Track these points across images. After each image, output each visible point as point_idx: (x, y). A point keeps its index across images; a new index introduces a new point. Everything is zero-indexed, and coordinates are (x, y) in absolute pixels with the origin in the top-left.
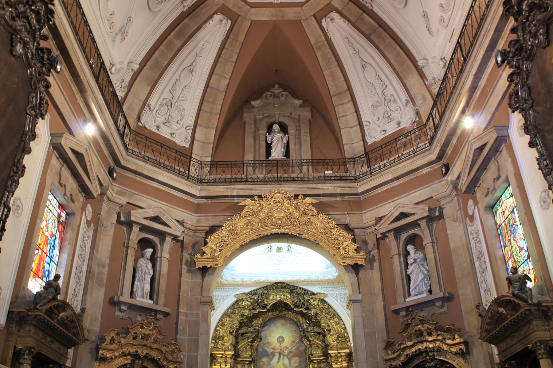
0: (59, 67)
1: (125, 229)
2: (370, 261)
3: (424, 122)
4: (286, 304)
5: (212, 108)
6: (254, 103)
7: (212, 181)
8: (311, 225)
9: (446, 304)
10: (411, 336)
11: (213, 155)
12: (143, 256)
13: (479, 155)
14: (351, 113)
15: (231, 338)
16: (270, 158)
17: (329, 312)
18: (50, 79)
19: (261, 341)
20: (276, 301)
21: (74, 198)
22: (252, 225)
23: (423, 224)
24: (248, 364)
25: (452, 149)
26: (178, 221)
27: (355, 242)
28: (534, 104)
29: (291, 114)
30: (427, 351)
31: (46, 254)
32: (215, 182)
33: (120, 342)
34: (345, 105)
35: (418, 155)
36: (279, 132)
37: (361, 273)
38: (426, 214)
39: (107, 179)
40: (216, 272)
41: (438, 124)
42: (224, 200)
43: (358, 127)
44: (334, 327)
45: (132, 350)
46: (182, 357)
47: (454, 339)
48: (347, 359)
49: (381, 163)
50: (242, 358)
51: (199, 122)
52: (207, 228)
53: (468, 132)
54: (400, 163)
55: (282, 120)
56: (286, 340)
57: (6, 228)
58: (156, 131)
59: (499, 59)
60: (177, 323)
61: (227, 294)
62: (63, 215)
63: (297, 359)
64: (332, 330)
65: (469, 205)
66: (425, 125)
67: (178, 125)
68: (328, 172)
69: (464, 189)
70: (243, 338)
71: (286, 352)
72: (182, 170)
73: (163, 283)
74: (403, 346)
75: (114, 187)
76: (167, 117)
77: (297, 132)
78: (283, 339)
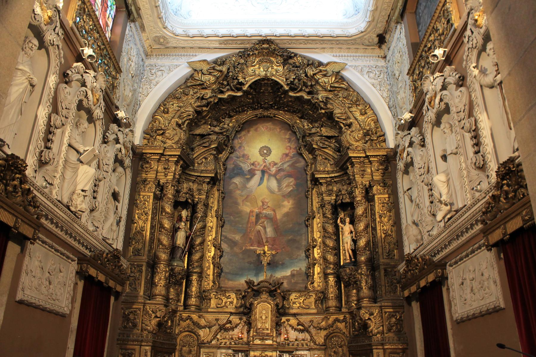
15: (178, 134)
17: (349, 95)
20: (259, 78)
24: (208, 183)
44: (356, 119)
48: (381, 167)
56: (274, 152)
64: (354, 125)
71: (273, 170)
78: (269, 151)
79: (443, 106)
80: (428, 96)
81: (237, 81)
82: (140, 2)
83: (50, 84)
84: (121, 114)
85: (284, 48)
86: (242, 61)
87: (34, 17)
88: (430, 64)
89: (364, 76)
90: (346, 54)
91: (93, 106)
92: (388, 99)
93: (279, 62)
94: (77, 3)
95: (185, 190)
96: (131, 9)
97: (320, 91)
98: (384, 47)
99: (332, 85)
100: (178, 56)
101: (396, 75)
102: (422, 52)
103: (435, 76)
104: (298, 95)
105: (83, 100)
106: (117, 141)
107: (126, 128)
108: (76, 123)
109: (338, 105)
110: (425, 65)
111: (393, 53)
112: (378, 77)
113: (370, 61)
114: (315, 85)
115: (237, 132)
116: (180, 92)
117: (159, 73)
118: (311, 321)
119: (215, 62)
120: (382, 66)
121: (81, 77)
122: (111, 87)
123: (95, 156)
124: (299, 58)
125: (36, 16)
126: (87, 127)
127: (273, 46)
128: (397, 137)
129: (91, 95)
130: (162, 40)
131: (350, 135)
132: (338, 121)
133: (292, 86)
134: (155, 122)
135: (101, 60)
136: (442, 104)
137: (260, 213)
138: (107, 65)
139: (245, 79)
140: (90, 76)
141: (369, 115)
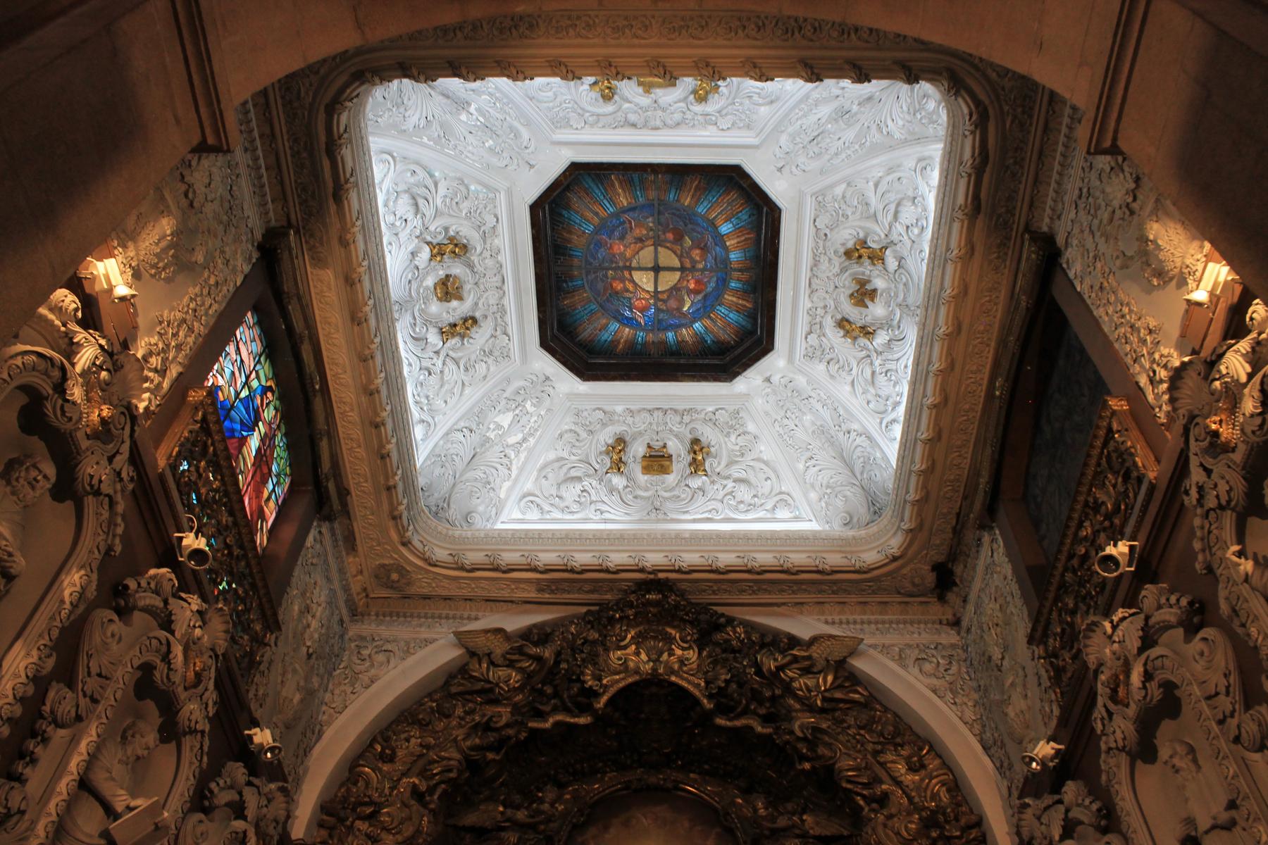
17: (872, 720)
20: (637, 678)
44: (898, 783)
79: (1156, 693)
80: (1103, 677)
81: (578, 685)
82: (350, 476)
83: (63, 591)
84: (262, 737)
85: (700, 604)
86: (594, 635)
87: (62, 407)
88: (1092, 598)
89: (909, 669)
90: (858, 618)
91: (180, 689)
92: (977, 727)
93: (689, 638)
94: (188, 424)
96: (327, 487)
97: (797, 711)
98: (950, 596)
99: (827, 694)
100: (433, 617)
101: (994, 658)
102: (1063, 575)
103: (1115, 619)
104: (738, 723)
105: (155, 668)
106: (238, 810)
107: (271, 780)
108: (125, 731)
109: (846, 747)
110: (1076, 605)
111: (978, 606)
112: (946, 670)
113: (920, 634)
114: (782, 696)
115: (575, 827)
116: (431, 708)
117: (381, 657)
119: (527, 635)
120: (953, 646)
121: (162, 605)
122: (246, 660)
123: (157, 827)
124: (738, 630)
125: (66, 405)
126: (152, 745)
127: (672, 598)
128: (1023, 816)
129: (180, 657)
130: (395, 576)
131: (885, 826)
132: (850, 790)
133: (723, 700)
134: (355, 784)
135: (229, 584)
136: (1153, 686)
138: (243, 601)
139: (600, 680)
140: (188, 608)
141: (931, 773)
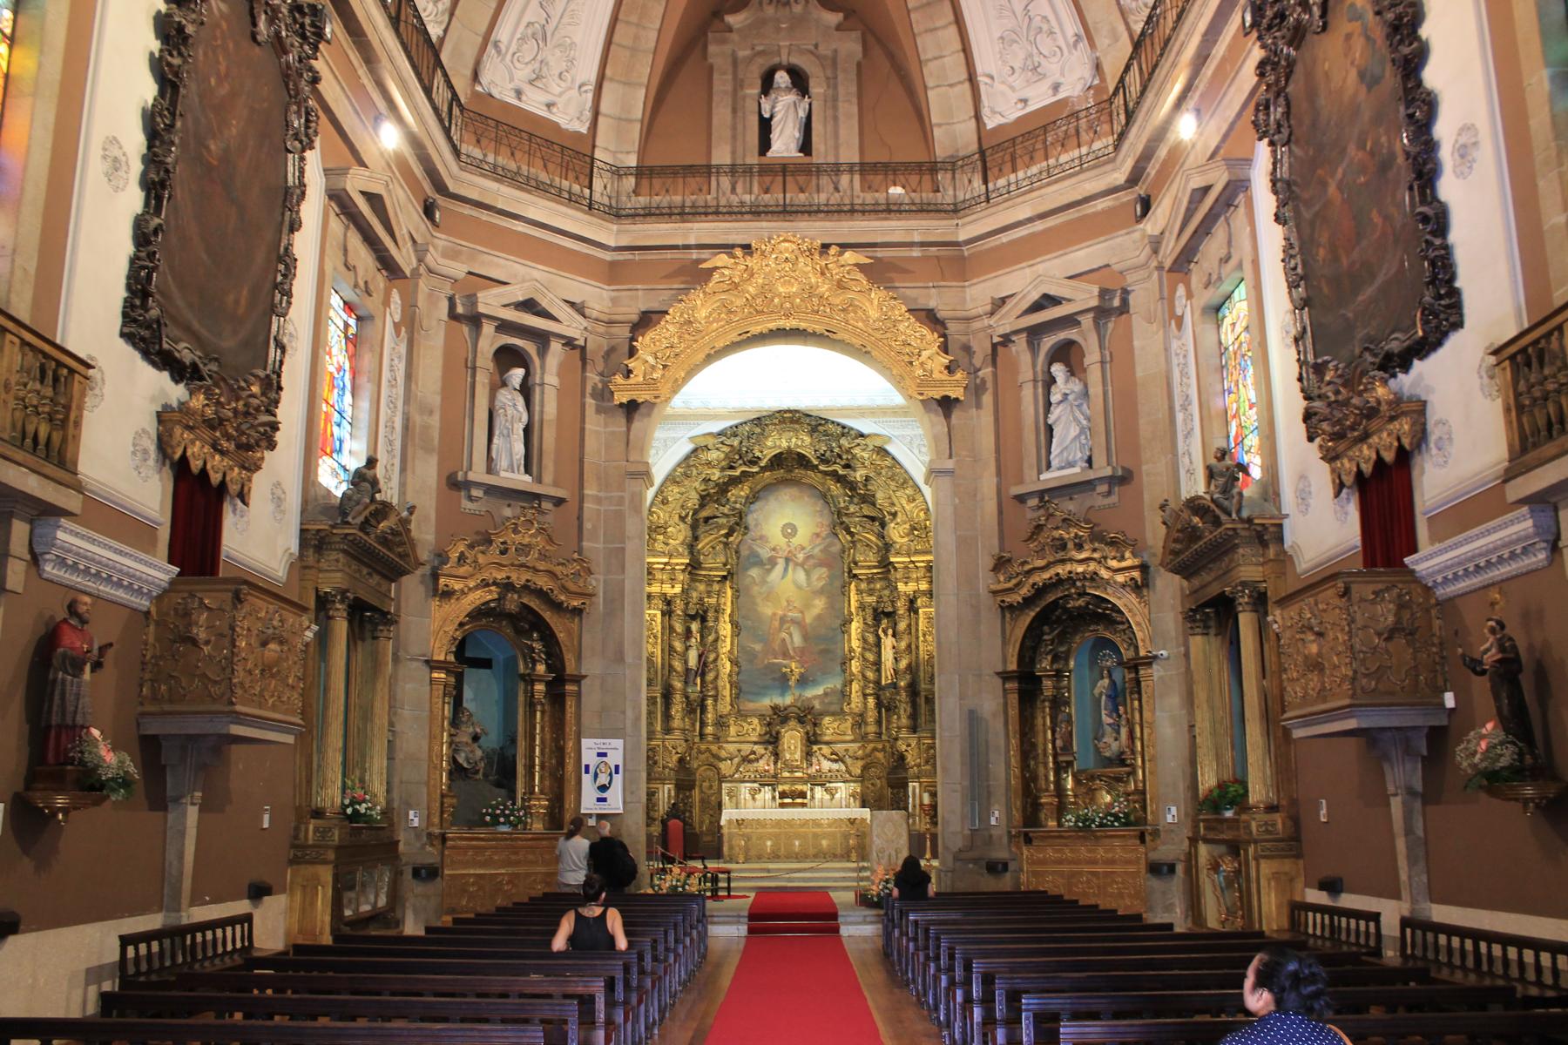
0: (328, 30)
1: (465, 329)
2: (976, 390)
3: (1111, 90)
4: (801, 457)
5: (637, 38)
6: (731, 19)
7: (642, 212)
8: (856, 313)
9: (1116, 489)
10: (1043, 549)
11: (642, 153)
12: (504, 384)
13: (1201, 201)
14: (953, 53)
16: (769, 154)
17: (894, 475)
18: (318, 65)
19: (745, 534)
21: (371, 287)
22: (730, 312)
23: (1087, 321)
25: (1157, 166)
26: (572, 304)
27: (947, 353)
28: (1293, 138)
29: (816, 46)
30: (1071, 580)
31: (333, 406)
32: (649, 214)
33: (475, 562)
34: (940, 33)
35: (1088, 169)
36: (790, 90)
37: (956, 415)
38: (1094, 303)
39: (423, 227)
40: (656, 410)
41: (1133, 112)
42: (669, 255)
43: (967, 85)
45: (500, 576)
46: (594, 583)
47: (1122, 558)
49: (1012, 177)
50: (705, 569)
51: (608, 72)
52: (635, 318)
53: (1186, 147)
54: (1049, 184)
55: (796, 60)
57: (283, 384)
58: (514, 102)
59: (1248, 19)
60: (580, 518)
61: (672, 434)
62: (352, 322)
63: (823, 571)
64: (899, 514)
65: (1178, 294)
66: (1110, 101)
67: (563, 84)
68: (896, 191)
69: (1168, 264)
70: (708, 528)
71: (801, 556)
72: (576, 188)
73: (549, 438)
74: (1027, 567)
75: (436, 241)
76: (537, 65)
77: (830, 92)
78: (794, 529)
95: (695, 601)
118: (847, 750)
137: (785, 615)
